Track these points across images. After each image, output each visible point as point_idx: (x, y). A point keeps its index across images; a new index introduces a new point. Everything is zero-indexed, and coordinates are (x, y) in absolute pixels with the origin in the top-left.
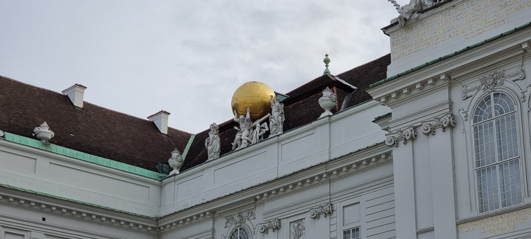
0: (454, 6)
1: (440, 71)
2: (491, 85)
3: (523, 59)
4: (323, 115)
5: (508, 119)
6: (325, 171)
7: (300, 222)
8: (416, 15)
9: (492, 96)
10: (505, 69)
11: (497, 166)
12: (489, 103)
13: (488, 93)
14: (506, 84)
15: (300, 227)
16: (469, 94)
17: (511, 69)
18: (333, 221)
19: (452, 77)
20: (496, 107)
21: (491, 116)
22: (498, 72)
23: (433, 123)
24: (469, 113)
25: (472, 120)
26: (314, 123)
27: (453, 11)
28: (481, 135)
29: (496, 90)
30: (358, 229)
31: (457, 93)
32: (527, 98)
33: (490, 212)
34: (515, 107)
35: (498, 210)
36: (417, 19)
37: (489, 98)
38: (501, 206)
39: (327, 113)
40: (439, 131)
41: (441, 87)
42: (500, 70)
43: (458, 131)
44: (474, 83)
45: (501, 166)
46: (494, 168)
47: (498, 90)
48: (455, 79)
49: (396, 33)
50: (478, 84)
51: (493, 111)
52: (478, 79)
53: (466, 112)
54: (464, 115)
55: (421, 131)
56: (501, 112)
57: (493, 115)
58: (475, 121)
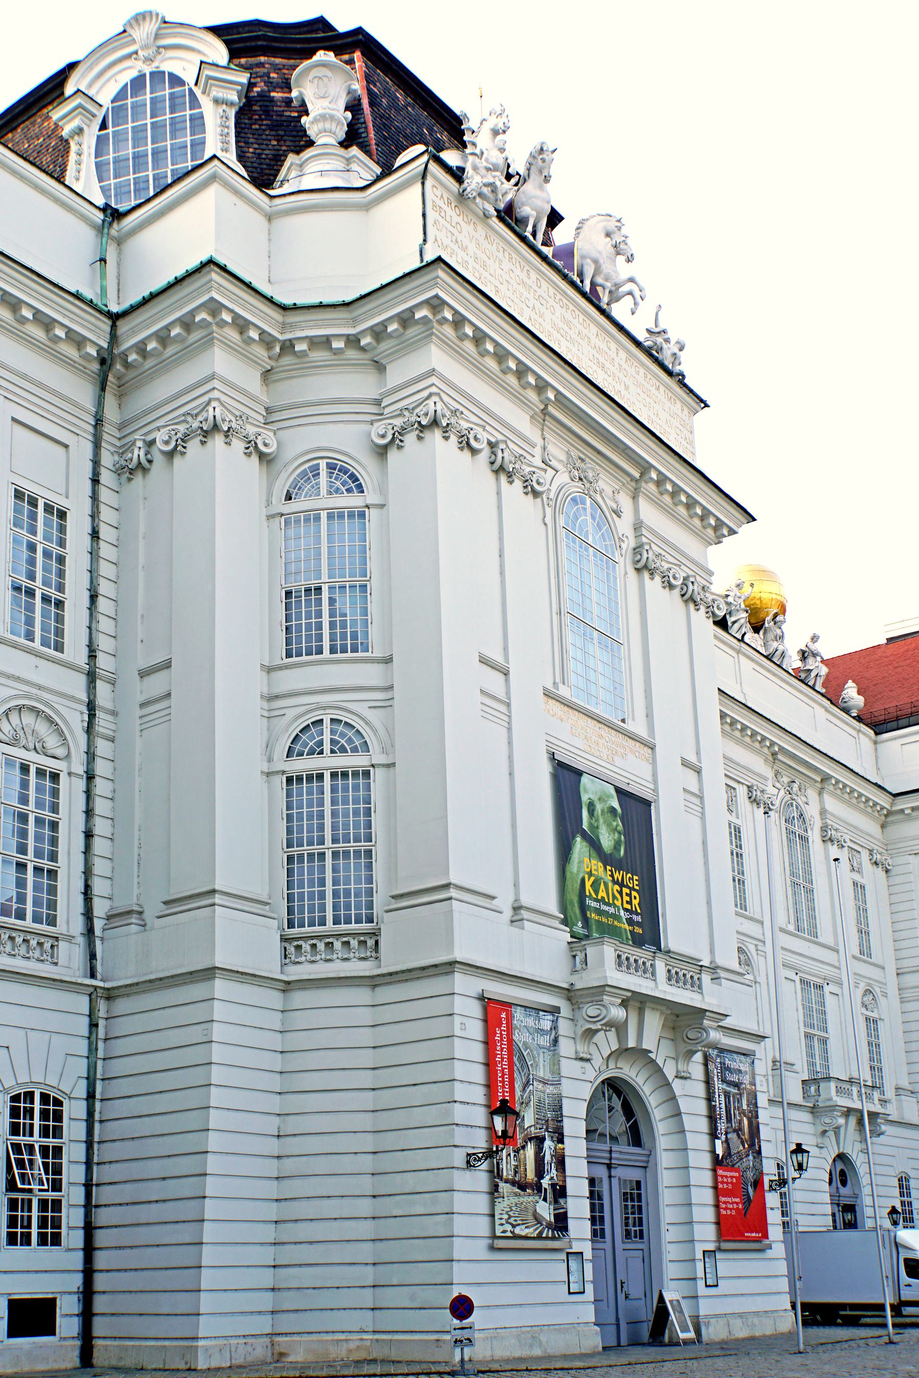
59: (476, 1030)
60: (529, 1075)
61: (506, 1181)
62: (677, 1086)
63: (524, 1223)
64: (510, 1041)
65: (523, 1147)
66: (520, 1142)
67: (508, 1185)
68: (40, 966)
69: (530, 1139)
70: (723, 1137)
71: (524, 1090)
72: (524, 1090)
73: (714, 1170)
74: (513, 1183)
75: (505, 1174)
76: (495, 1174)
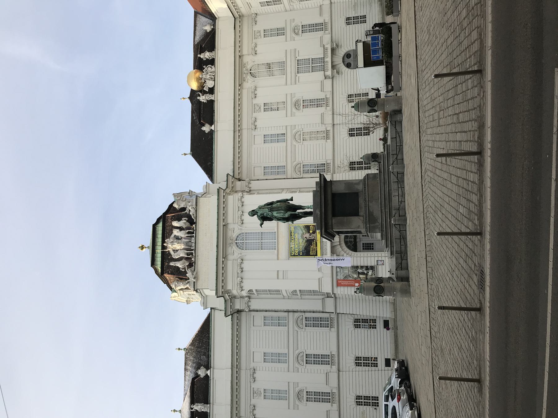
0: (198, 256)
1: (221, 259)
4: (209, 375)
6: (235, 369)
7: (254, 392)
8: (195, 273)
11: (262, 241)
12: (239, 243)
14: (234, 236)
15: (256, 393)
16: (232, 252)
17: (230, 233)
18: (258, 369)
19: (225, 257)
20: (241, 240)
21: (243, 243)
26: (211, 378)
27: (199, 257)
28: (249, 247)
30: (265, 353)
31: (230, 257)
32: (241, 228)
36: (196, 273)
39: (208, 372)
41: (226, 264)
42: (228, 238)
44: (230, 250)
45: (262, 240)
46: (262, 242)
47: (235, 239)
48: (225, 256)
49: (198, 285)
53: (239, 254)
57: (243, 241)
68: (335, 320)
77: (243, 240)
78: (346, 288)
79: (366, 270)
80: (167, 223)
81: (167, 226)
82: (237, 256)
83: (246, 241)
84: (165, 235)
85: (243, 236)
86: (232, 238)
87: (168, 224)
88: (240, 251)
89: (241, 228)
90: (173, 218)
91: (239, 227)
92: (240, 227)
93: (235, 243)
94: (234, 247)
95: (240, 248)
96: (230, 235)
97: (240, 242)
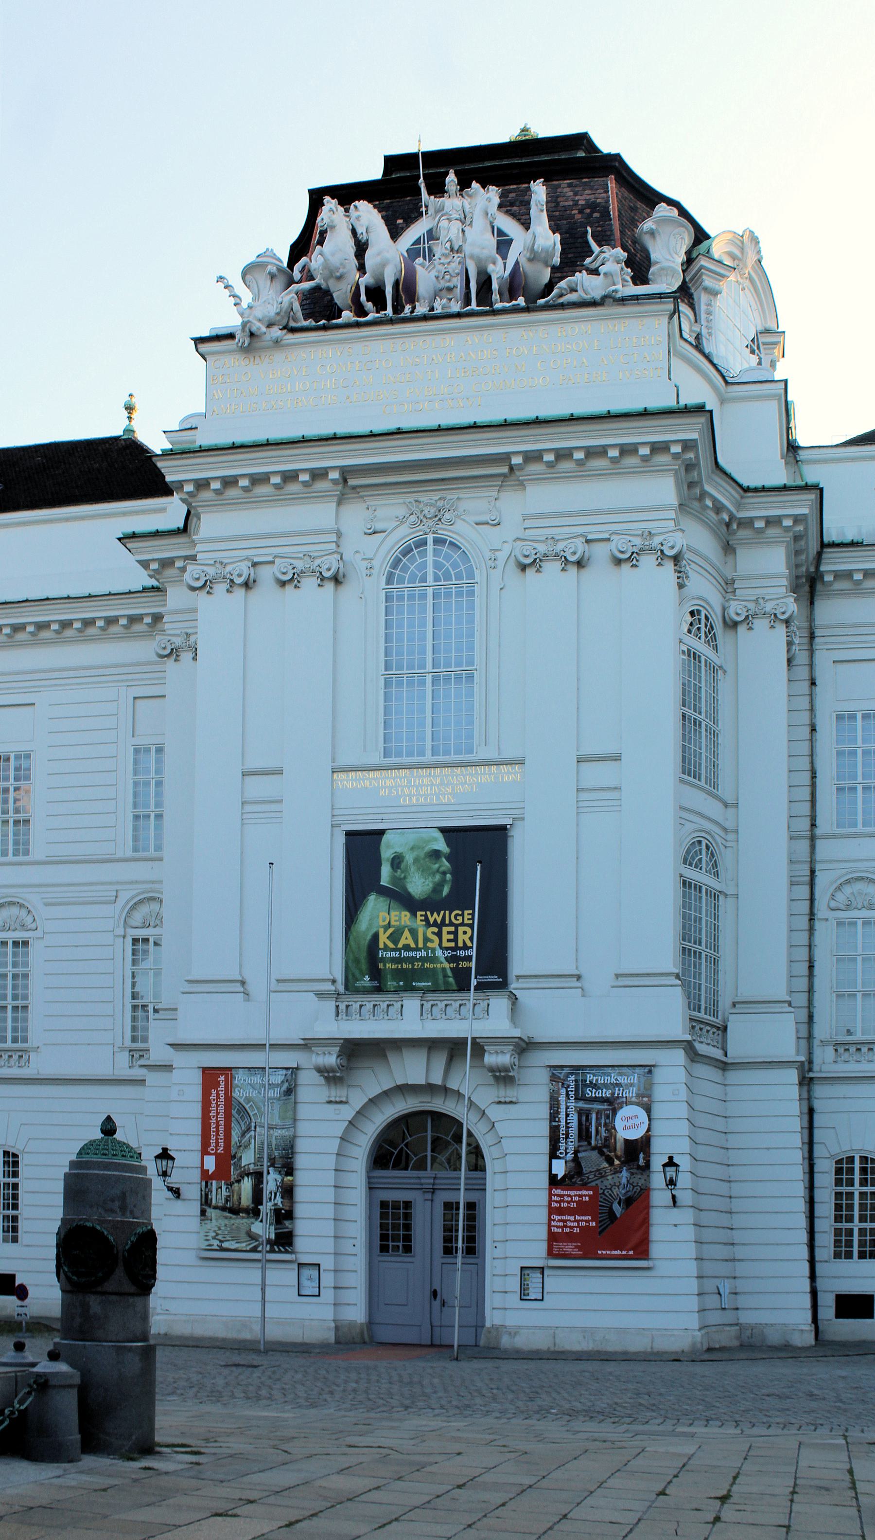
2: (430, 518)
3: (501, 486)
5: (459, 594)
9: (430, 541)
10: (461, 496)
12: (424, 554)
13: (421, 533)
14: (459, 526)
16: (379, 526)
20: (437, 565)
21: (424, 579)
22: (449, 497)
23: (300, 565)
24: (376, 563)
25: (383, 579)
28: (400, 612)
29: (439, 532)
32: (500, 563)
33: (406, 760)
34: (477, 573)
35: (421, 759)
37: (424, 543)
38: (428, 752)
40: (309, 583)
42: (452, 496)
43: (348, 591)
47: (443, 533)
50: (401, 511)
51: (430, 570)
52: (401, 501)
53: (371, 559)
54: (365, 563)
55: (266, 574)
56: (448, 577)
58: (389, 581)
59: (196, 1093)
60: (250, 1123)
61: (215, 1208)
62: (495, 1112)
63: (234, 1239)
64: (229, 1099)
65: (239, 1181)
66: (234, 1177)
67: (217, 1211)
69: (248, 1175)
70: (570, 1156)
71: (243, 1135)
72: (243, 1135)
73: (550, 1190)
74: (223, 1209)
75: (214, 1202)
76: (206, 1201)
77: (437, 578)
78: (196, 1110)
79: (277, 1212)
80: (570, 185)
81: (559, 186)
82: (357, 552)
83: (430, 591)
84: (512, 187)
85: (459, 577)
86: (447, 516)
87: (568, 189)
88: (382, 565)
89: (500, 563)
90: (596, 215)
91: (507, 548)
92: (502, 556)
93: (418, 534)
94: (403, 534)
95: (396, 563)
96: (463, 505)
97: (424, 565)
